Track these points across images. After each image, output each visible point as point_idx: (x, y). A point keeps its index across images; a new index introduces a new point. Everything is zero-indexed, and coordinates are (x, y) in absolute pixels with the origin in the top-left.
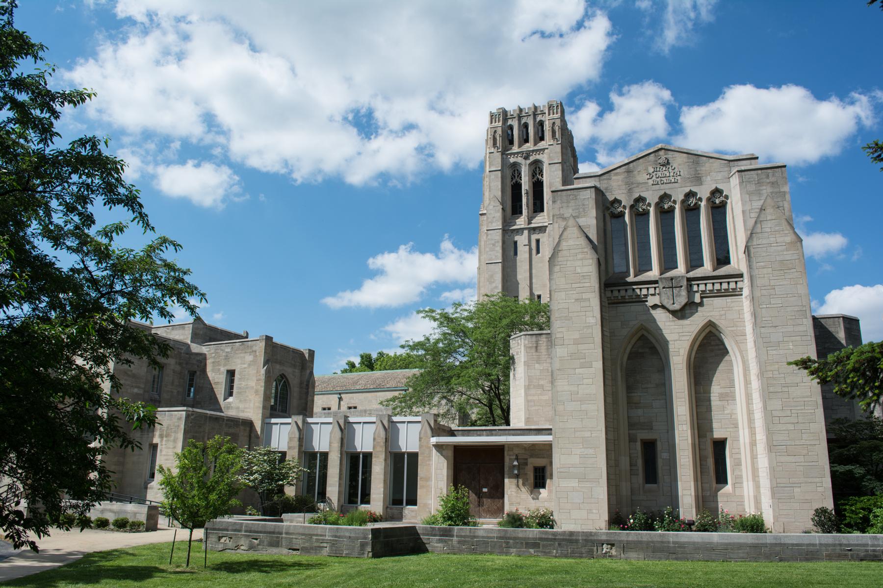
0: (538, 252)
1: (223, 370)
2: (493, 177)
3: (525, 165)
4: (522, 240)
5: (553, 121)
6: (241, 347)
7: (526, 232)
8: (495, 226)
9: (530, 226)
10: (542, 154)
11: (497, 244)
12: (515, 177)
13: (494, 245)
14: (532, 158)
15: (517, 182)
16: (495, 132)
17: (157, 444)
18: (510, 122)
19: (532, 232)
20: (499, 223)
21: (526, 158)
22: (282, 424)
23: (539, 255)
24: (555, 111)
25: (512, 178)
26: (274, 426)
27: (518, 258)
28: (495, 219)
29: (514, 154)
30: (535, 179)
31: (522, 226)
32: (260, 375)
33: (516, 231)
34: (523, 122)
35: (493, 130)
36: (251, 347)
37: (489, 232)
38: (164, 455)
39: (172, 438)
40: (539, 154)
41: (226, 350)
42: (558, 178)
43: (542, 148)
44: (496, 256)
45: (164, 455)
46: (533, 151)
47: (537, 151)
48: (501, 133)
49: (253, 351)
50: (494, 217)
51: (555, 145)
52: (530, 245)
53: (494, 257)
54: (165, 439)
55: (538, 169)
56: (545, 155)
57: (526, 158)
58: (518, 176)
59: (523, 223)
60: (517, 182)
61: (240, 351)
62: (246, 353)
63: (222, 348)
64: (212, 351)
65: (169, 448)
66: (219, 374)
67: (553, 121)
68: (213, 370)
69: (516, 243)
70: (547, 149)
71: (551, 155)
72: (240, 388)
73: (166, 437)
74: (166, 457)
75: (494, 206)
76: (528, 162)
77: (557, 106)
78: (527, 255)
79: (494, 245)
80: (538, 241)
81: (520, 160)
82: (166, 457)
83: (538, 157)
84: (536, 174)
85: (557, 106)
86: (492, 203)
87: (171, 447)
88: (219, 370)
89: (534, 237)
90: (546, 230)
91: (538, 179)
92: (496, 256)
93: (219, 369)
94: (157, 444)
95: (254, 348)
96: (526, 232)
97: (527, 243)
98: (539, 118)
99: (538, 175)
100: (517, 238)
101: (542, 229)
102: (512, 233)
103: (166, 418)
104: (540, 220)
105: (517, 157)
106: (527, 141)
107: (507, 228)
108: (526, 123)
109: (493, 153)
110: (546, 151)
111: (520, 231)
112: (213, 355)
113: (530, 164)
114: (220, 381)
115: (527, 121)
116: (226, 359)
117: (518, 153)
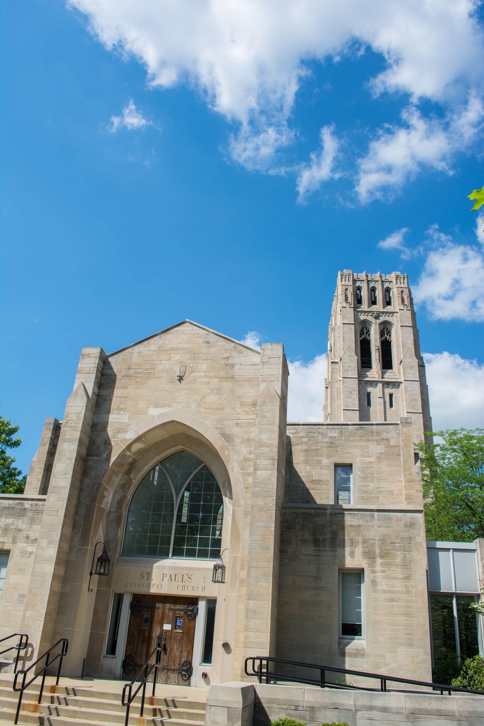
0: (391, 406)
1: (328, 462)
2: (346, 329)
3: (376, 323)
4: (376, 392)
5: (402, 289)
6: (359, 432)
7: (380, 385)
8: (351, 375)
9: (383, 380)
10: (392, 316)
11: (353, 392)
12: (363, 333)
13: (350, 392)
14: (382, 319)
15: (365, 338)
16: (346, 289)
17: (362, 570)
18: (358, 284)
19: (386, 386)
20: (354, 373)
21: (377, 318)
22: (455, 550)
23: (392, 408)
24: (402, 281)
25: (361, 334)
26: (440, 553)
27: (372, 408)
28: (350, 369)
29: (365, 312)
30: (383, 338)
31: (376, 379)
32: (411, 474)
33: (370, 383)
34: (371, 285)
35: (345, 288)
36: (378, 433)
37: (345, 379)
38: (385, 592)
39: (399, 560)
40: (388, 316)
41: (330, 434)
42: (410, 340)
43: (392, 311)
44: (352, 404)
45: (385, 592)
46: (383, 313)
47: (387, 313)
48: (352, 291)
49: (382, 439)
50: (349, 366)
51: (405, 310)
52: (384, 397)
53: (350, 405)
54: (379, 561)
55: (386, 330)
56: (394, 318)
57: (377, 318)
58: (367, 333)
59: (377, 376)
60: (365, 338)
61: (358, 438)
62: (368, 440)
63: (320, 430)
64: (302, 434)
65: (395, 578)
66: (320, 469)
67: (402, 289)
68: (306, 462)
69: (369, 394)
70: (397, 313)
71: (402, 318)
72: (366, 492)
73: (382, 557)
74: (387, 596)
75: (349, 356)
76: (378, 321)
77: (404, 278)
78: (382, 407)
79: (350, 392)
80: (391, 396)
81: (370, 318)
82: (387, 596)
83: (387, 318)
84: (384, 334)
85: (404, 278)
86: (347, 353)
87: (400, 576)
88: (319, 462)
89: (388, 391)
90: (399, 386)
91: (386, 339)
92: (352, 404)
93: (321, 460)
94: (362, 570)
95: (385, 435)
96: (380, 385)
97: (381, 396)
98: (386, 285)
99: (386, 335)
100: (369, 389)
101: (396, 385)
102: (366, 384)
103: (376, 522)
104: (389, 376)
105: (367, 315)
106: (374, 303)
107: (361, 379)
108: (373, 287)
109: (345, 307)
110: (395, 314)
111: (373, 383)
112: (305, 440)
113: (380, 324)
114: (324, 478)
115: (375, 286)
116: (330, 447)
117: (368, 312)
